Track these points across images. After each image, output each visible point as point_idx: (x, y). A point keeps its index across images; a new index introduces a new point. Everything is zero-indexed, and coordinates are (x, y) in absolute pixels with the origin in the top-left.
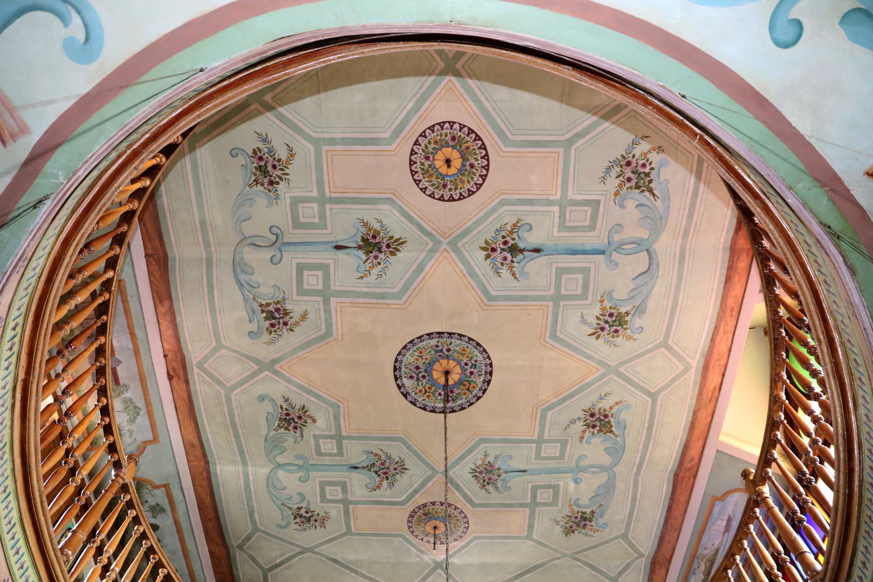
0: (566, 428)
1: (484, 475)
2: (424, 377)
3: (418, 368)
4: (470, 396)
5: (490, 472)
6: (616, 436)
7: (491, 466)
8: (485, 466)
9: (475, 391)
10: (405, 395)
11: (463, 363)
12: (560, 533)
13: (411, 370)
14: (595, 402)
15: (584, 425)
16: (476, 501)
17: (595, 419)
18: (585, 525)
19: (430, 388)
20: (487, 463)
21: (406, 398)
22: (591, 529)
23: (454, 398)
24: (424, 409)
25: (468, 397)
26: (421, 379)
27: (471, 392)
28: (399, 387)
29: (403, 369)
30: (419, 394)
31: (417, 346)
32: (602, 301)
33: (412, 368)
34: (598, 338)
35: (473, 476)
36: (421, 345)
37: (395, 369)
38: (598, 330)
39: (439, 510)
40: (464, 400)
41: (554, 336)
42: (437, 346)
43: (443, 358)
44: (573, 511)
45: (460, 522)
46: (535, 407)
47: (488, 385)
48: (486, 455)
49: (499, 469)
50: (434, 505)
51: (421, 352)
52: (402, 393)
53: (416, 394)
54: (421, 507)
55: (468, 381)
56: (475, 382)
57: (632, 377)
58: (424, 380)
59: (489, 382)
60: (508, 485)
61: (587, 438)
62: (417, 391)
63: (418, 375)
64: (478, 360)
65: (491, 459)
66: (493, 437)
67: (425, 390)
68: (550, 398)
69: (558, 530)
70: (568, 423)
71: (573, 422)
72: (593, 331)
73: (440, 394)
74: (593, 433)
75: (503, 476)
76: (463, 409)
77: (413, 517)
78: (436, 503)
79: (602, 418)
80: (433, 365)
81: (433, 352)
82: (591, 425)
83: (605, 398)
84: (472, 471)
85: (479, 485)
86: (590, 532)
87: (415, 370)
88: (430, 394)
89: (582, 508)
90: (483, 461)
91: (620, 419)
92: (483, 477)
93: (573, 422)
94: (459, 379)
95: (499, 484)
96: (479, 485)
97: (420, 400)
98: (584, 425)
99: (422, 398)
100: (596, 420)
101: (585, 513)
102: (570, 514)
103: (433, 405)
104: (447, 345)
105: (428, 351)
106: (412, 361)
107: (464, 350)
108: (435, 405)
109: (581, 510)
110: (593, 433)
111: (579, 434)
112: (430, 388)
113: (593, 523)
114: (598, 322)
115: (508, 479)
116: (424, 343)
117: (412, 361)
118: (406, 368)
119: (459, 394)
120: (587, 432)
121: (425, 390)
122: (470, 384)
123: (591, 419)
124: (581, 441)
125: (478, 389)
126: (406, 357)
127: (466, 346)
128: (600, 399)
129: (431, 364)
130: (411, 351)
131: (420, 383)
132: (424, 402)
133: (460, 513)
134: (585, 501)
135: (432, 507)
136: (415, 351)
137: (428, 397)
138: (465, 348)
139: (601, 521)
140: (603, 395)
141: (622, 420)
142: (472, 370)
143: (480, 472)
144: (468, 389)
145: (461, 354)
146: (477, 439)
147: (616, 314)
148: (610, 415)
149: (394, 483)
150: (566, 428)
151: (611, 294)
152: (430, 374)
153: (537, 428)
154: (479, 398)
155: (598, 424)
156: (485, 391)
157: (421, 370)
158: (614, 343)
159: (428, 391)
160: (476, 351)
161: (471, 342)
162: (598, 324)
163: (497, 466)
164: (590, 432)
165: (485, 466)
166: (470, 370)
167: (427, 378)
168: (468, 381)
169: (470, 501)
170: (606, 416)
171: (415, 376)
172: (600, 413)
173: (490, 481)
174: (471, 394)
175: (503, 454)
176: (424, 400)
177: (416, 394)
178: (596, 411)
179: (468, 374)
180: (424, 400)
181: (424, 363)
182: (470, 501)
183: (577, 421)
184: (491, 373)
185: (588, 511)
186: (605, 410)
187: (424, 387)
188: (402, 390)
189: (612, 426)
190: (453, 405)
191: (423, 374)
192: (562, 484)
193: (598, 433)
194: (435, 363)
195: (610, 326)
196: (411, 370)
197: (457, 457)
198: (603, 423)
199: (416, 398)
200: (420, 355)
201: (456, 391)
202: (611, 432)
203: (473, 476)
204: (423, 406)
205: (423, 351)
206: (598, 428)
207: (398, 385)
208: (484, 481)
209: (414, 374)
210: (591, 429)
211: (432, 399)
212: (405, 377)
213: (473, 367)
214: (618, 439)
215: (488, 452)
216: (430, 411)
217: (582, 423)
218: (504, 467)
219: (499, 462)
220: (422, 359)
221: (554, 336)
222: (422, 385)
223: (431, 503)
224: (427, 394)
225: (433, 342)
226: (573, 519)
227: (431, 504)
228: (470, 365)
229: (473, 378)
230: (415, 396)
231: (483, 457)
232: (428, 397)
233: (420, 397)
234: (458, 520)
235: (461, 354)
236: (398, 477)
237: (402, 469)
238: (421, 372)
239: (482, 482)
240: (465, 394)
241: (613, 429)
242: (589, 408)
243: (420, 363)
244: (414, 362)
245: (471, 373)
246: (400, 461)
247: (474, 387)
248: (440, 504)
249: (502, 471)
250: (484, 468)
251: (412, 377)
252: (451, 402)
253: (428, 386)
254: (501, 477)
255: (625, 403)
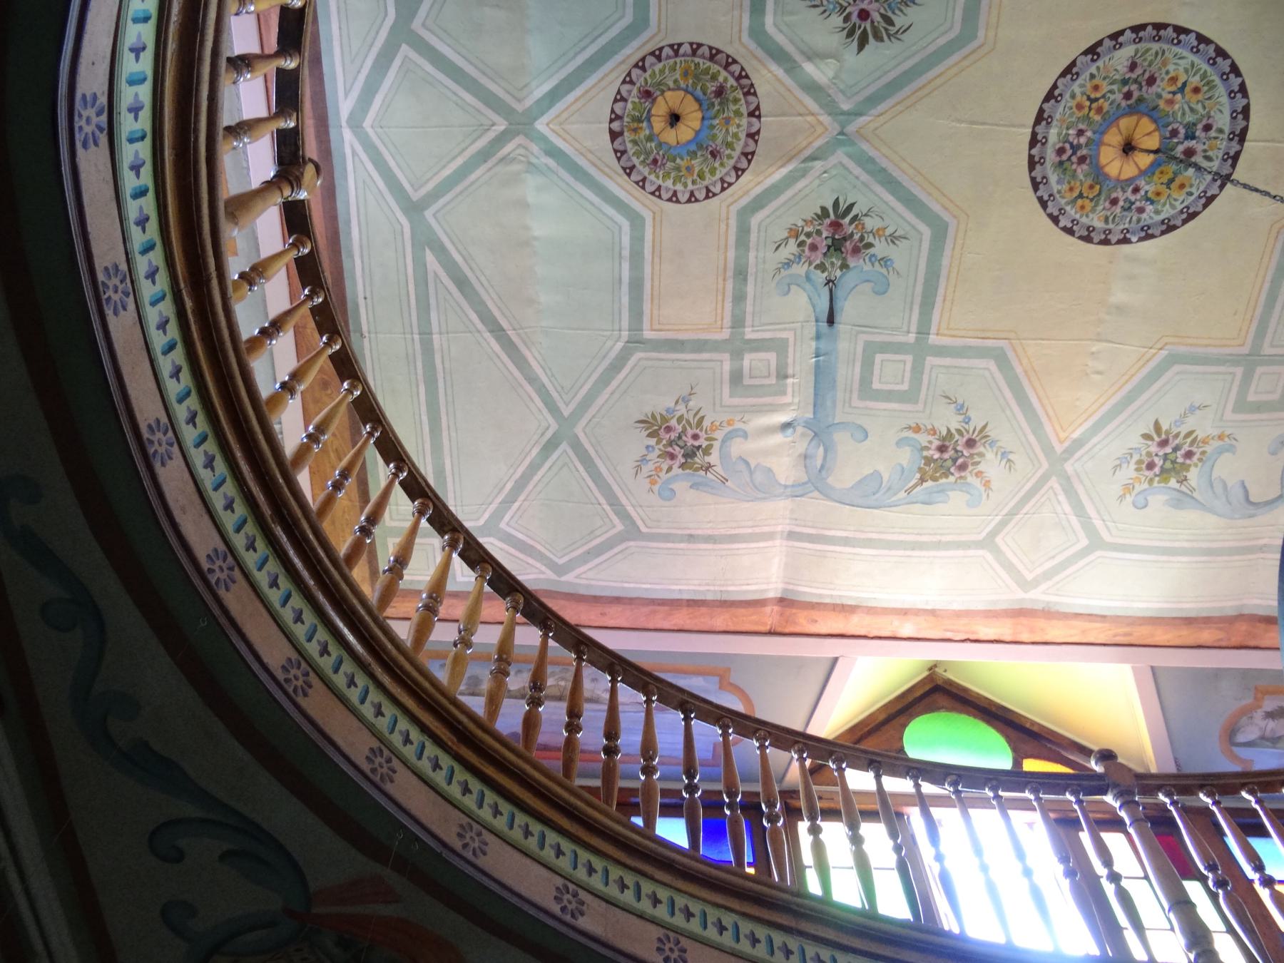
0: (947, 397)
1: (824, 235)
2: (1128, 96)
3: (1151, 81)
4: (1063, 201)
5: (836, 246)
6: (909, 491)
7: (856, 251)
8: (856, 237)
9: (1073, 212)
10: (1093, 51)
11: (1141, 183)
12: (648, 410)
13: (1150, 65)
14: (999, 444)
15: (949, 430)
16: (755, 221)
17: (959, 448)
18: (672, 457)
19: (1099, 110)
20: (870, 239)
21: (1085, 53)
22: (658, 469)
23: (1067, 165)
24: (1050, 96)
25: (1063, 197)
26: (1125, 89)
27: (1074, 201)
28: (1115, 36)
29: (1155, 46)
30: (1089, 85)
31: (1217, 81)
32: (1220, 437)
33: (1154, 68)
34: (1147, 437)
35: (824, 209)
36: (1221, 91)
37: (1159, 27)
38: (1163, 436)
39: (733, 129)
40: (1055, 187)
41: (1173, 360)
42: (1208, 128)
43: (1163, 138)
44: (714, 428)
45: (694, 182)
46: (1012, 335)
47: (1081, 238)
48: (893, 239)
49: (844, 266)
50: (751, 114)
51: (1196, 90)
52: (1100, 43)
53: (1092, 76)
54: (744, 81)
55: (1099, 194)
56: (1093, 210)
57: (1034, 501)
58: (1121, 96)
59: (1087, 239)
60: (792, 287)
61: (913, 439)
62: (1096, 81)
63: (1136, 81)
64: (1144, 216)
65: (880, 248)
66: (947, 252)
67: (1096, 100)
68: (1025, 361)
69: (660, 403)
70: (960, 401)
71: (961, 409)
72: (1165, 427)
73: (1081, 133)
74: (927, 448)
75: (820, 277)
76: (1035, 185)
77: (712, 58)
78: (754, 120)
79: (960, 461)
80: (1151, 117)
81: (1190, 118)
82: (947, 443)
83: (1005, 461)
84: (842, 207)
85: (800, 223)
86: (648, 468)
87: (1147, 75)
88: (1086, 110)
89: (723, 441)
90: (877, 233)
91: (949, 493)
92: (819, 233)
93: (961, 409)
94: (1107, 177)
95: (800, 269)
96: (800, 223)
97: (1076, 88)
98: (949, 430)
99: (1077, 90)
100: (957, 451)
101: (707, 451)
102: (706, 423)
103: (1058, 116)
104: (1205, 151)
105: (1199, 107)
106: (1171, 67)
107: (1182, 186)
108: (1055, 123)
109: (716, 444)
110: (927, 448)
111: (925, 422)
112: (1099, 110)
113: (676, 470)
114: (1182, 435)
115: (808, 286)
116: (1225, 99)
117: (1171, 67)
118: (1157, 53)
119: (1074, 176)
120: (931, 438)
121: (1096, 100)
122: (1091, 200)
123: (962, 441)
124: (909, 428)
125: (1077, 216)
126: (1186, 53)
127: (1193, 190)
128: (1004, 454)
129: (1153, 113)
130: (1205, 67)
131: (1115, 87)
132: (1067, 96)
133: (722, 180)
134: (738, 448)
135: (744, 110)
136: (1204, 76)
137: (1080, 107)
138: (1187, 189)
139: (681, 486)
140: (1011, 457)
141: (948, 495)
142: (1121, 203)
143: (836, 225)
144: (1081, 196)
145: (1171, 181)
146: (946, 217)
147: (1188, 462)
148: (963, 474)
149: (821, 9)
150: (947, 397)
151: (1227, 451)
152: (1132, 111)
153: (958, 342)
154: (1055, 220)
155: (946, 456)
156: (1070, 231)
157: (1144, 88)
158: (1125, 466)
159: (1095, 105)
160: (1173, 212)
161: (1203, 200)
162: (1177, 436)
163: (852, 262)
164: (930, 442)
165: (856, 237)
166: (1122, 199)
167: (1124, 103)
168: (1099, 194)
169: (758, 203)
170: (963, 467)
171: (1134, 76)
172: (972, 455)
173: (806, 249)
174: (1068, 203)
175: (892, 277)
176: (1073, 96)
177: (1092, 76)
178: (980, 448)
179: (1114, 195)
180: (1073, 96)
181: (1159, 96)
182: (758, 203)
183: (961, 418)
184: (1106, 242)
185: (713, 458)
186: (978, 463)
187: (1103, 96)
188: (1108, 43)
189: (935, 479)
190: (1048, 164)
191: (1136, 95)
192: (788, 399)
193: (926, 458)
194: (1155, 121)
195: (1166, 454)
196: (1150, 65)
197: (896, 173)
198: (949, 463)
199: (1082, 78)
200: (1187, 89)
201: (1081, 171)
202: (922, 480)
203: (824, 209)
204: (1057, 92)
205: (1200, 96)
206: (937, 456)
207: (1121, 33)
208: (808, 235)
209: (1139, 71)
210: (936, 443)
211: (1072, 115)
212: (1137, 52)
213: (1127, 205)
214: (902, 494)
215: (903, 244)
216: (1041, 111)
217: (954, 426)
218: (850, 279)
219: (868, 267)
220: (1174, 93)
221: (1173, 360)
222: (1111, 92)
223: (758, 108)
224: (1088, 103)
225: (1223, 120)
226: (690, 432)
227: (752, 107)
228: (1133, 198)
229: (1103, 204)
230: (1085, 76)
231: (888, 232)
232: (1080, 107)
233: (1082, 86)
234: (701, 176)
235: (1171, 181)
236: (837, 20)
237: (865, 31)
238: (1140, 88)
239: (807, 229)
240: (1071, 189)
241: (929, 484)
242: (988, 436)
243: (1163, 88)
244: (1167, 73)
245: (1114, 202)
246: (893, 30)
247: (1082, 207)
248: (754, 130)
249: (838, 273)
250: (852, 235)
251: (1133, 67)
252: (1058, 159)
253: (1106, 106)
254: (819, 272)
255: (984, 496)
